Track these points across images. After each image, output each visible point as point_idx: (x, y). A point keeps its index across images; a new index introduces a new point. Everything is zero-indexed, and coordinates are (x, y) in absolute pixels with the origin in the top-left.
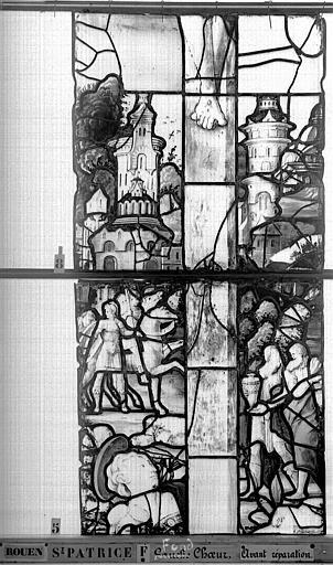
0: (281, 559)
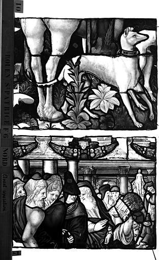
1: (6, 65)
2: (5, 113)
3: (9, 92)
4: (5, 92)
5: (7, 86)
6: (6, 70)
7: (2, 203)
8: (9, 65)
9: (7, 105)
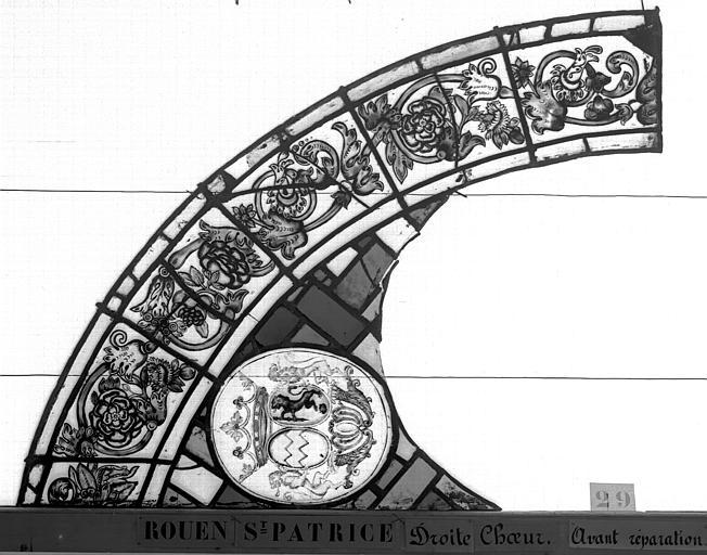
0: (648, 547)
1: (182, 536)
2: (352, 539)
3: (276, 525)
4: (276, 538)
5: (254, 534)
6: (199, 537)
7: (673, 547)
8: (182, 524)
9: (324, 533)
